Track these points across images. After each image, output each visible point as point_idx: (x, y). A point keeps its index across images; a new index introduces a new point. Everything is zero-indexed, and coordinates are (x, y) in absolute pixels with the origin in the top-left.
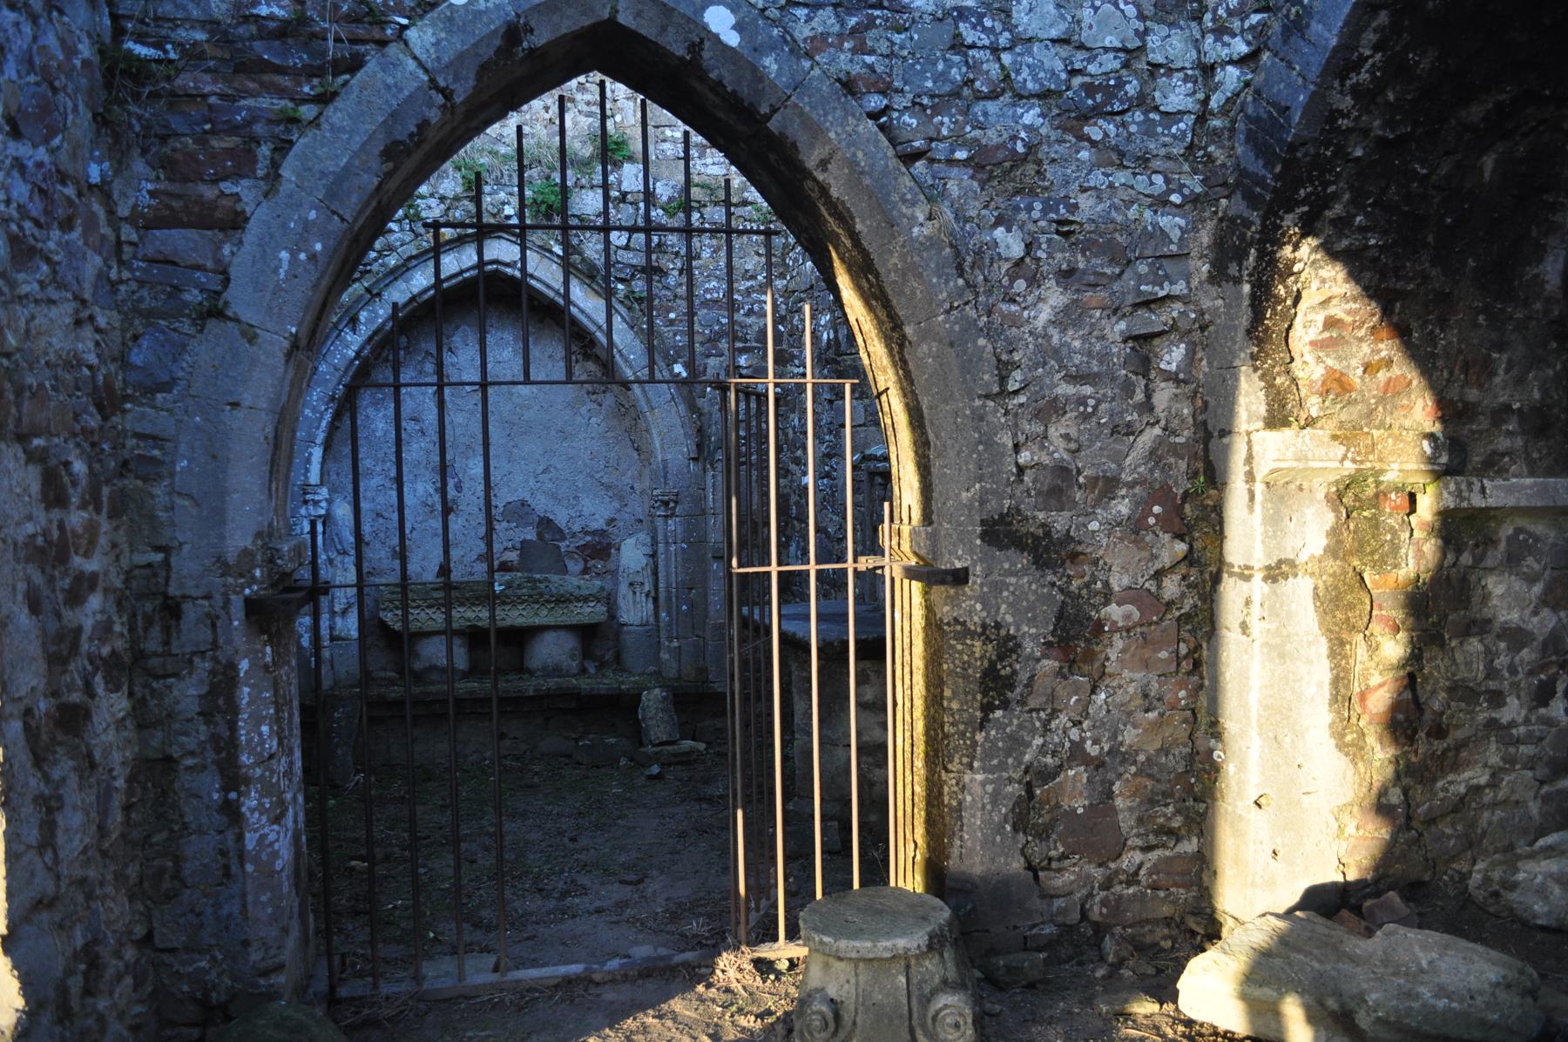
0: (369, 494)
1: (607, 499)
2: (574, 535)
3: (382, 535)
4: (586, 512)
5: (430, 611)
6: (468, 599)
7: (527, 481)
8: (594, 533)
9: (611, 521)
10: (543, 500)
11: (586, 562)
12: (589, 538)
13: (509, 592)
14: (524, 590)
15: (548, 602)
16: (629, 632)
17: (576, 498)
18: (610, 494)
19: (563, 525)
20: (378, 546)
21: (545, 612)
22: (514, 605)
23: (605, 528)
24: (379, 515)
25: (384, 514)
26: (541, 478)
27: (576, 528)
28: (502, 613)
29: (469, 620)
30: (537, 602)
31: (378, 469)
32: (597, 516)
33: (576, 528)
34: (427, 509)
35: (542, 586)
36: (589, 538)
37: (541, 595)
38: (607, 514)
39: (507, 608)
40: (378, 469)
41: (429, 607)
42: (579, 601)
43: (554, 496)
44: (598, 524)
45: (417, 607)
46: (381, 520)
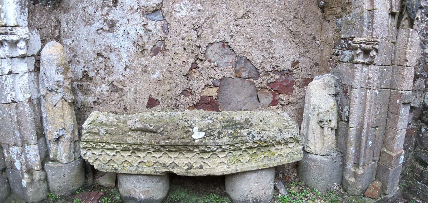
0: (91, 37)
1: (294, 45)
2: (267, 73)
3: (102, 72)
4: (277, 55)
5: (126, 154)
6: (163, 147)
7: (228, 24)
8: (281, 72)
9: (295, 64)
10: (242, 43)
11: (274, 96)
12: (277, 77)
13: (209, 141)
14: (225, 140)
15: (250, 148)
16: (314, 161)
17: (269, 42)
18: (296, 41)
19: (258, 66)
20: (99, 81)
21: (247, 158)
22: (214, 153)
23: (291, 69)
24: (99, 55)
25: (104, 53)
26: (240, 22)
27: (269, 68)
28: (200, 161)
29: (165, 166)
30: (239, 149)
31: (98, 14)
32: (285, 59)
33: (269, 68)
34: (138, 49)
35: (244, 132)
36: (277, 77)
37: (243, 143)
38: (293, 58)
39: (206, 156)
40: (98, 14)
41: (124, 150)
42: (279, 143)
43: (251, 39)
44: (286, 65)
45: (113, 149)
46: (101, 59)
